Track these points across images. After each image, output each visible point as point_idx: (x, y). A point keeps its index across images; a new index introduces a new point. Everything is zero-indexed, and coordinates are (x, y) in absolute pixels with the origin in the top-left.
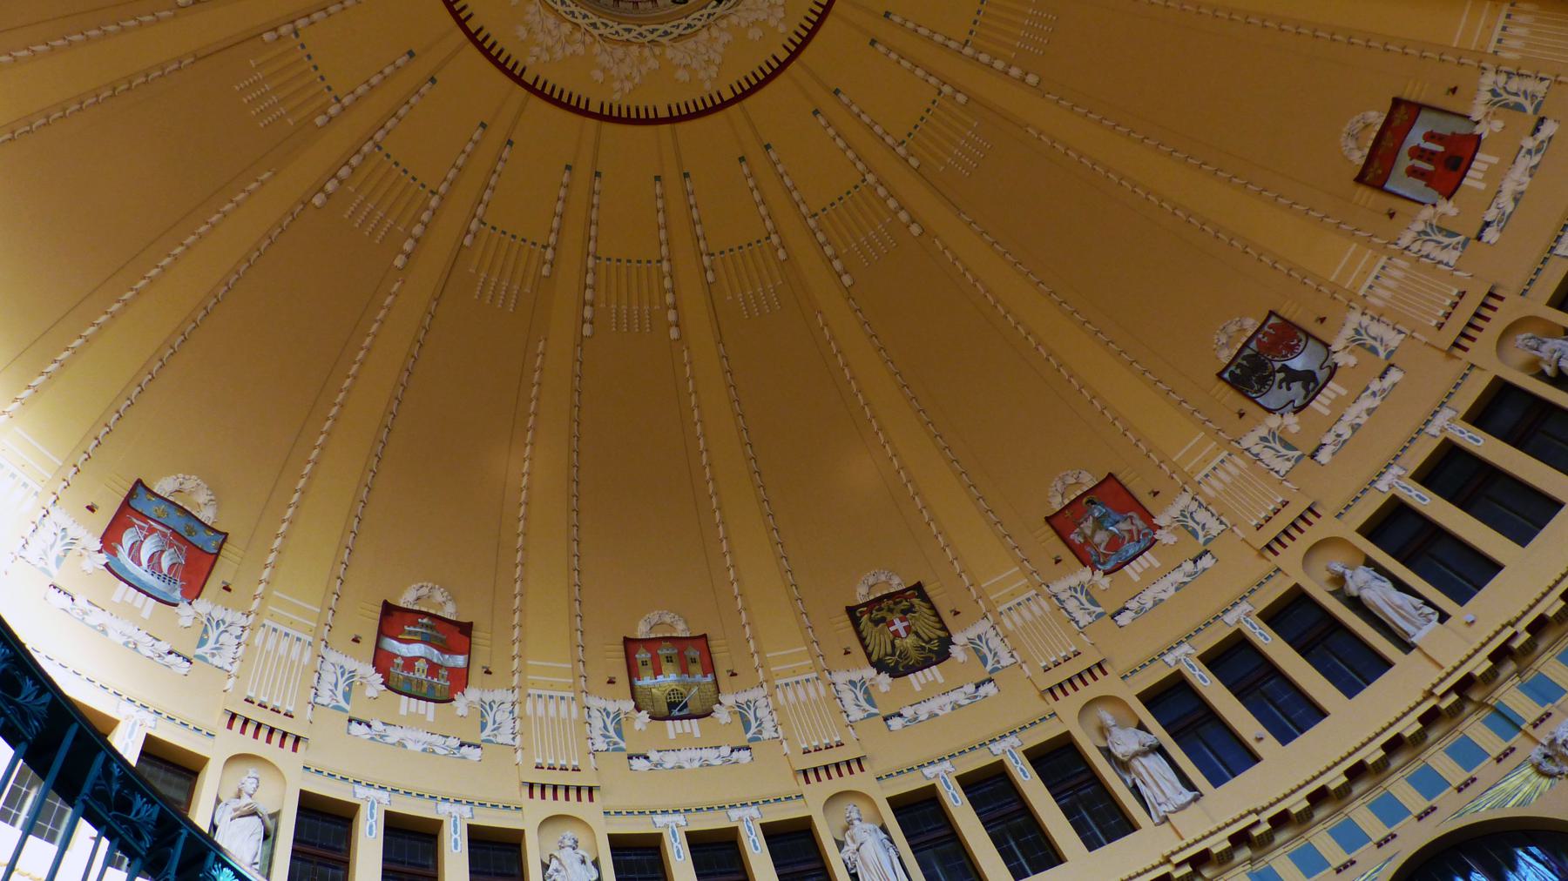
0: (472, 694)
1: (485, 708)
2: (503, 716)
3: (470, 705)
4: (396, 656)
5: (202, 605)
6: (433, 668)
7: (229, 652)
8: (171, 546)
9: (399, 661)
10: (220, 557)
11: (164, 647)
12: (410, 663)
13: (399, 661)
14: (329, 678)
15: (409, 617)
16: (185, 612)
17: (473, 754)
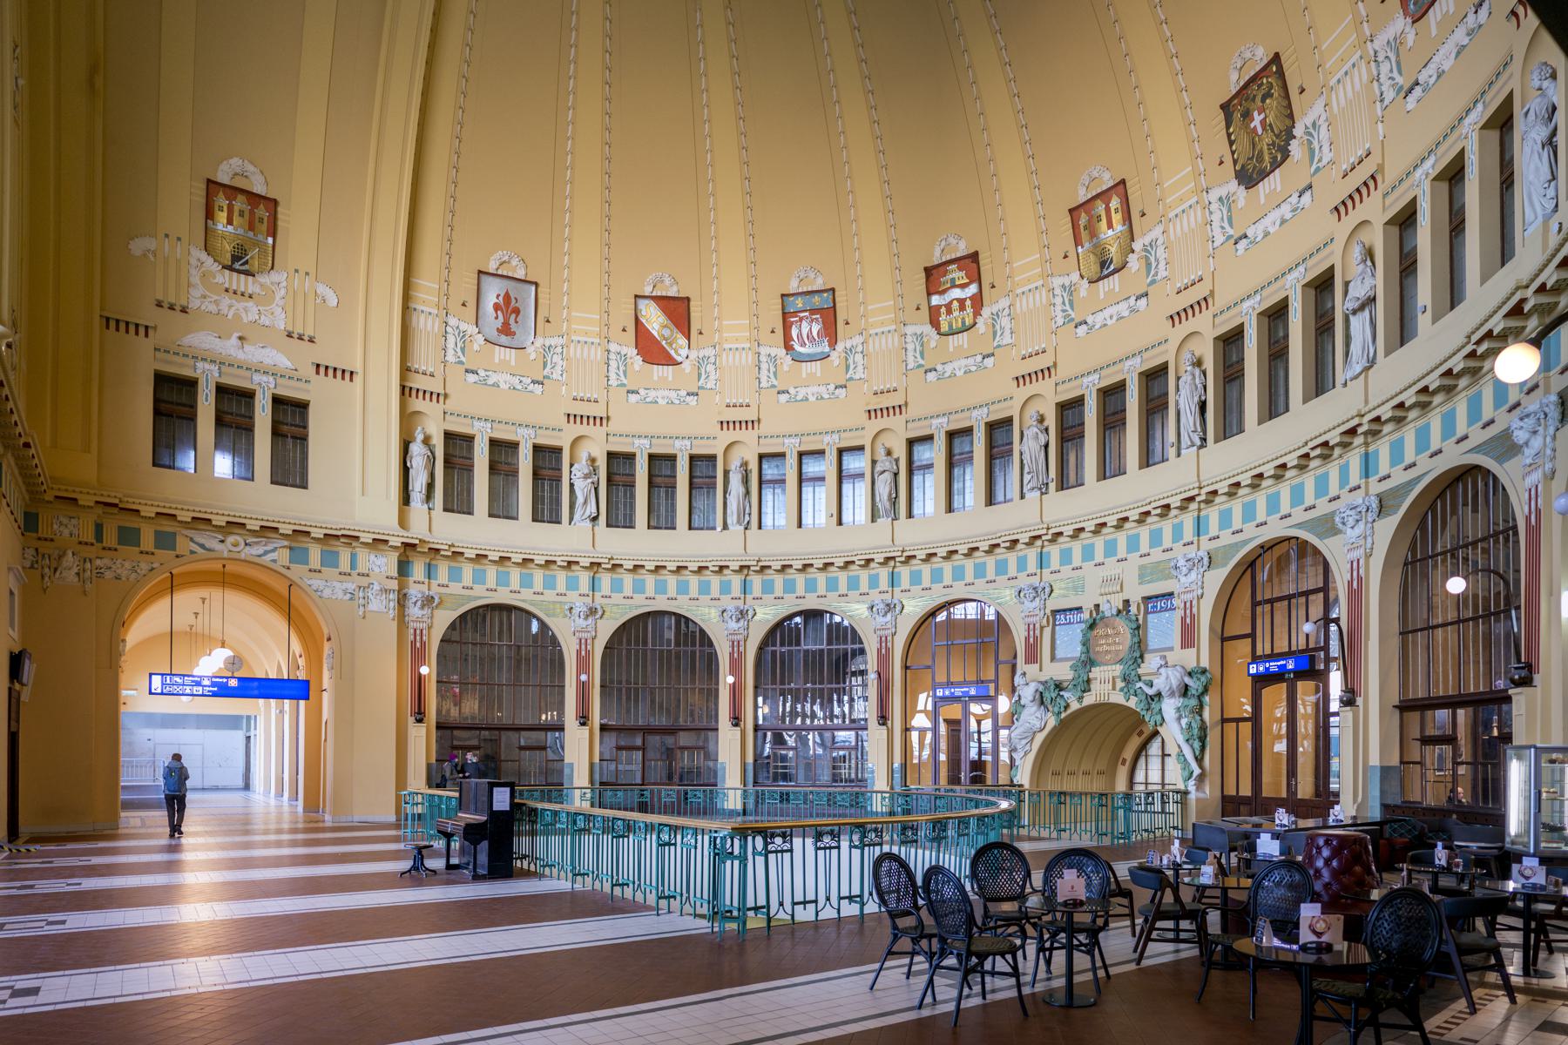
0: (986, 312)
1: (996, 316)
2: (1005, 322)
3: (986, 324)
4: (940, 306)
5: (840, 346)
6: (962, 302)
7: (860, 368)
8: (812, 321)
9: (943, 310)
10: (838, 305)
11: (832, 387)
12: (949, 307)
13: (943, 310)
14: (910, 347)
15: (941, 269)
16: (834, 355)
17: (989, 362)
